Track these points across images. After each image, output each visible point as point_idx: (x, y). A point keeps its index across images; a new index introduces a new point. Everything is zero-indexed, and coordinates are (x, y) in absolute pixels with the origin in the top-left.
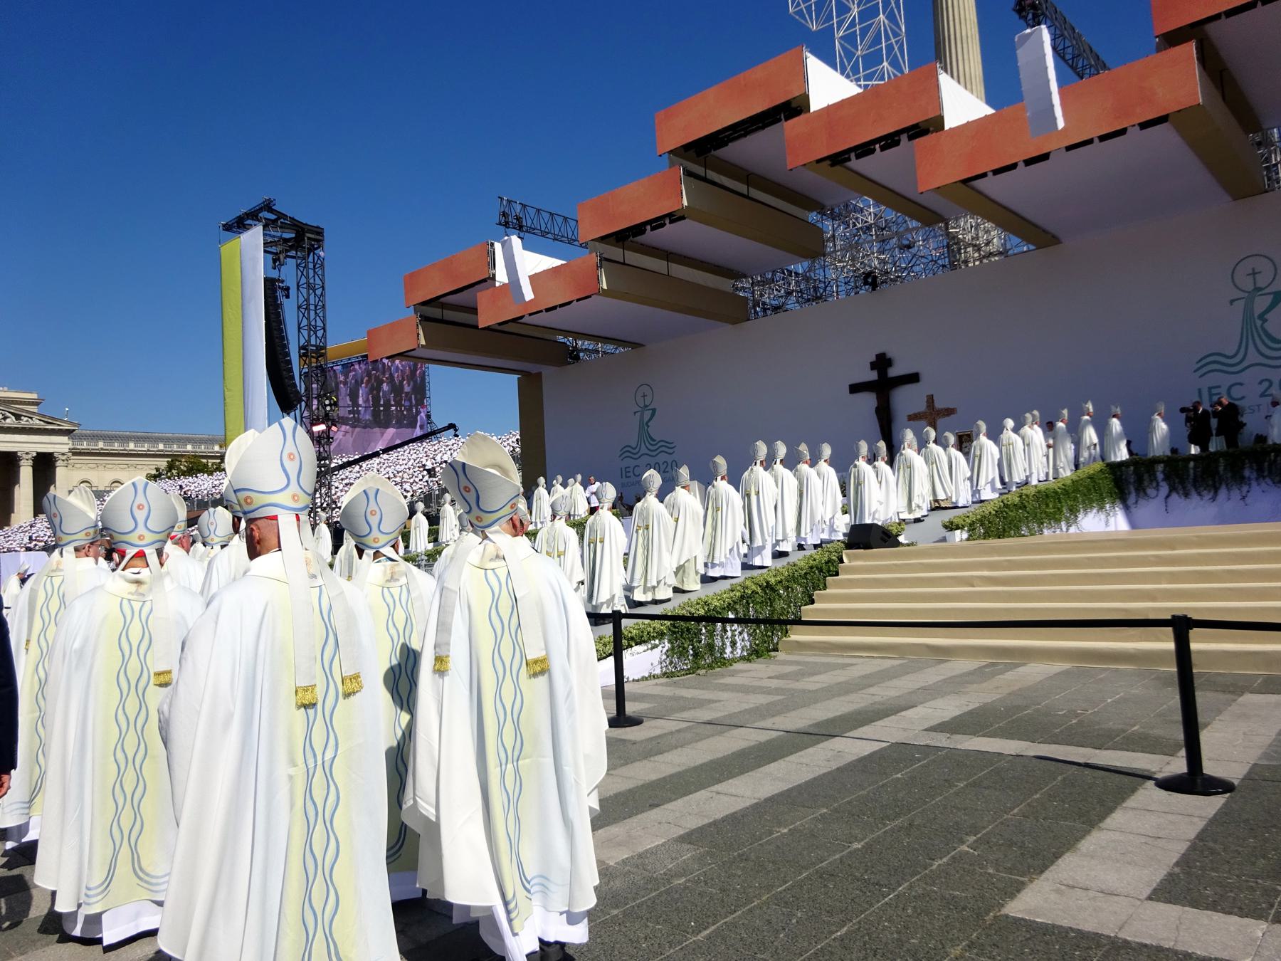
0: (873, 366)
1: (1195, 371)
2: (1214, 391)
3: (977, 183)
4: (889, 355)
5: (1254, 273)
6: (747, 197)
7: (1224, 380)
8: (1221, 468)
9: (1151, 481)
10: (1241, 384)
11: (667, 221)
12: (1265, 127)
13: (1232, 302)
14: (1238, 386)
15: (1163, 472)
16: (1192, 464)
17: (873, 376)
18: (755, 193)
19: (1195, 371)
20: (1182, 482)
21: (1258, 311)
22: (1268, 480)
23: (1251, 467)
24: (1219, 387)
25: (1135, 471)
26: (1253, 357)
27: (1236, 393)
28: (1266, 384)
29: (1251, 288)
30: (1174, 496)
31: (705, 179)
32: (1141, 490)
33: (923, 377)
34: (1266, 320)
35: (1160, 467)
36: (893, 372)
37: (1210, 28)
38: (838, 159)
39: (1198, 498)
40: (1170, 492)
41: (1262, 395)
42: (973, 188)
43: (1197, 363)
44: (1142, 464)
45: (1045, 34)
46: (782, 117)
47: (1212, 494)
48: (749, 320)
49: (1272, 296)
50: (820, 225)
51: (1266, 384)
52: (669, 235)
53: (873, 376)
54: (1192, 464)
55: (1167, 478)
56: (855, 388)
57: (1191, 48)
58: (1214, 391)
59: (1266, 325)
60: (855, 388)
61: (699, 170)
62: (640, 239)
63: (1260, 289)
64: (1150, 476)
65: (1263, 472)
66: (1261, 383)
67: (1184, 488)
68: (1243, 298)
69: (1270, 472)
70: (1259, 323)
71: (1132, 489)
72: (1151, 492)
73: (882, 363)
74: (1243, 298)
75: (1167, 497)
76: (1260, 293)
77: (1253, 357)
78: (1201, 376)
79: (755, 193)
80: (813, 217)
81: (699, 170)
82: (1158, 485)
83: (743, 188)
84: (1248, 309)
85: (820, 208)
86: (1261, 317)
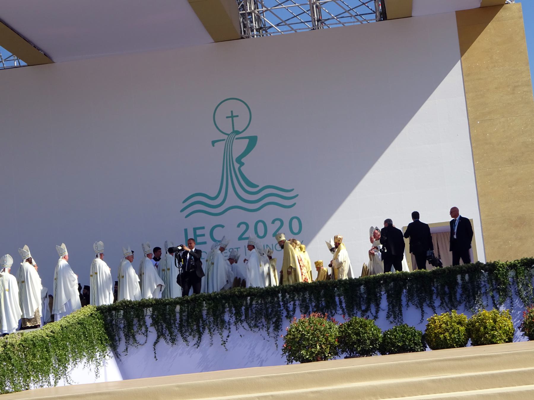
1: (182, 211)
2: (199, 232)
5: (232, 117)
7: (208, 221)
8: (204, 313)
9: (141, 326)
10: (223, 226)
13: (214, 143)
14: (220, 228)
15: (152, 316)
16: (178, 308)
19: (182, 211)
20: (169, 328)
22: (245, 324)
23: (230, 311)
24: (203, 228)
26: (232, 200)
27: (218, 234)
28: (243, 227)
29: (229, 131)
30: (162, 340)
32: (130, 336)
34: (242, 164)
35: (149, 312)
39: (185, 343)
40: (159, 337)
41: (241, 238)
43: (184, 202)
44: (132, 308)
47: (196, 339)
49: (247, 140)
51: (243, 227)
54: (178, 308)
55: (155, 323)
58: (199, 232)
59: (242, 168)
63: (238, 133)
64: (139, 321)
65: (241, 316)
66: (239, 226)
67: (171, 333)
68: (224, 140)
69: (246, 317)
70: (237, 166)
71: (122, 335)
72: (140, 338)
74: (224, 140)
75: (156, 343)
76: (237, 136)
77: (232, 200)
78: (186, 217)
82: (147, 331)
84: (228, 152)
86: (239, 160)
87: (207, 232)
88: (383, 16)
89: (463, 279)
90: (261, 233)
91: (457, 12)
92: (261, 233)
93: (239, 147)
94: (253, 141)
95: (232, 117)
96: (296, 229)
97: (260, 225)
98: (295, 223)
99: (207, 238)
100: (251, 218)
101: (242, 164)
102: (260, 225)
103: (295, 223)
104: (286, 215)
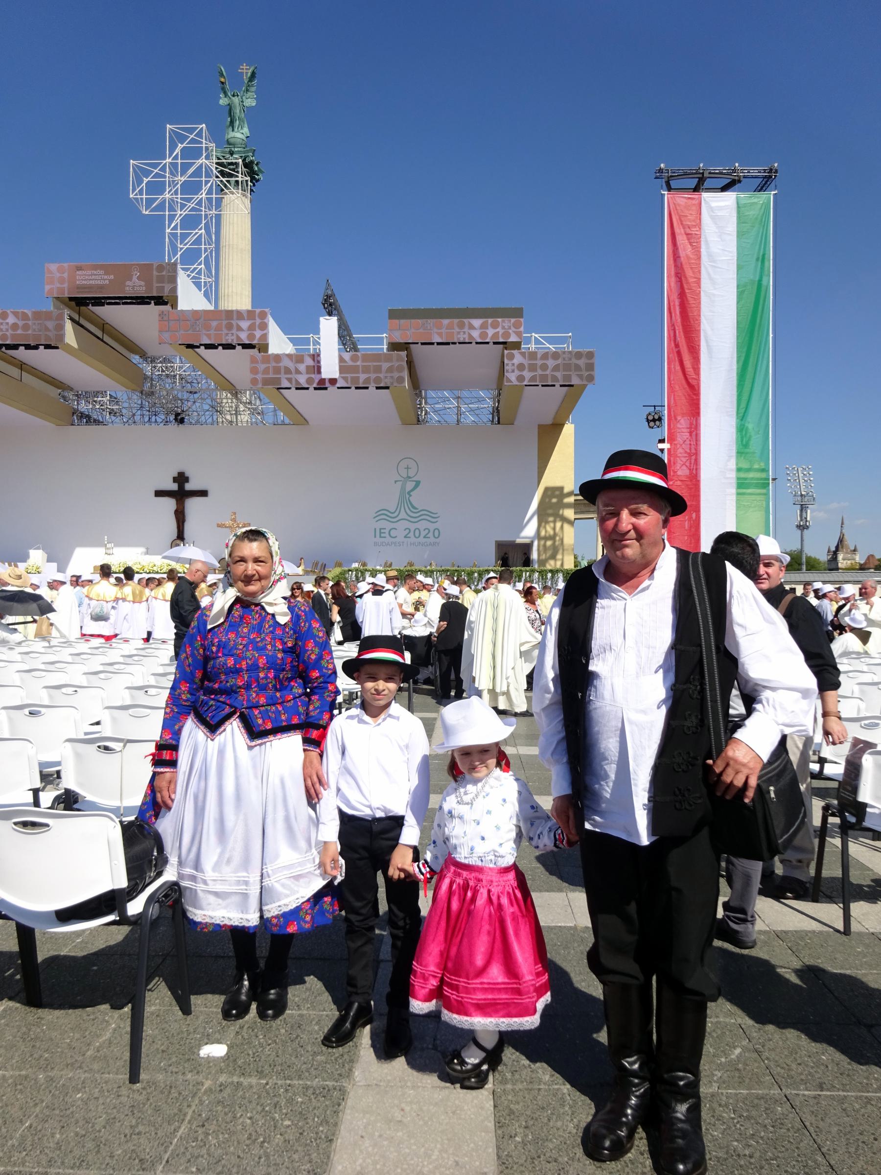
0: (175, 480)
2: (382, 531)
3: (281, 390)
4: (186, 475)
5: (408, 468)
6: (102, 340)
7: (387, 525)
11: (42, 347)
12: (421, 388)
13: (396, 482)
17: (174, 487)
18: (106, 338)
21: (408, 489)
25: (356, 576)
26: (403, 515)
27: (393, 533)
28: (408, 531)
31: (78, 323)
33: (209, 493)
34: (410, 496)
36: (188, 487)
37: (411, 345)
38: (190, 346)
41: (405, 537)
42: (280, 393)
45: (334, 320)
46: (152, 302)
48: (73, 425)
49: (415, 483)
50: (141, 366)
51: (408, 531)
52: (40, 358)
53: (174, 487)
56: (159, 493)
57: (404, 354)
58: (382, 531)
60: (159, 493)
61: (76, 317)
62: (11, 352)
63: (410, 478)
70: (407, 496)
73: (181, 478)
77: (403, 515)
79: (106, 338)
80: (136, 359)
81: (76, 317)
83: (99, 333)
84: (403, 488)
85: (143, 355)
86: (409, 493)
87: (387, 531)
88: (499, 423)
89: (526, 575)
90: (417, 534)
91: (539, 425)
92: (417, 535)
93: (410, 485)
94: (418, 483)
95: (408, 468)
96: (436, 535)
97: (417, 531)
98: (436, 531)
99: (387, 535)
100: (412, 527)
101: (410, 496)
102: (417, 531)
103: (436, 531)
104: (432, 527)
